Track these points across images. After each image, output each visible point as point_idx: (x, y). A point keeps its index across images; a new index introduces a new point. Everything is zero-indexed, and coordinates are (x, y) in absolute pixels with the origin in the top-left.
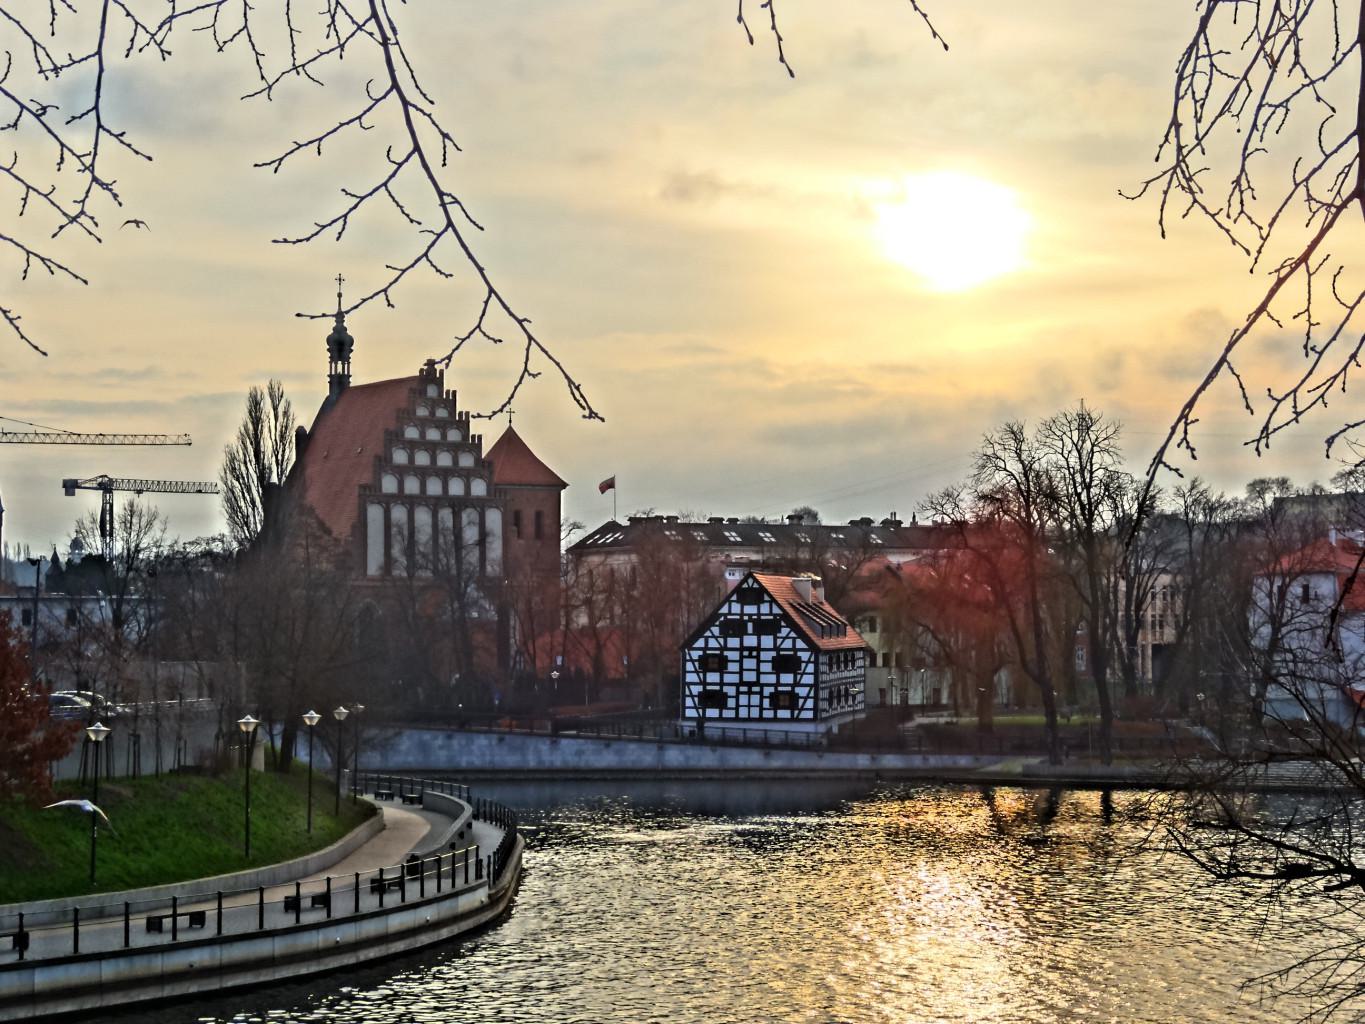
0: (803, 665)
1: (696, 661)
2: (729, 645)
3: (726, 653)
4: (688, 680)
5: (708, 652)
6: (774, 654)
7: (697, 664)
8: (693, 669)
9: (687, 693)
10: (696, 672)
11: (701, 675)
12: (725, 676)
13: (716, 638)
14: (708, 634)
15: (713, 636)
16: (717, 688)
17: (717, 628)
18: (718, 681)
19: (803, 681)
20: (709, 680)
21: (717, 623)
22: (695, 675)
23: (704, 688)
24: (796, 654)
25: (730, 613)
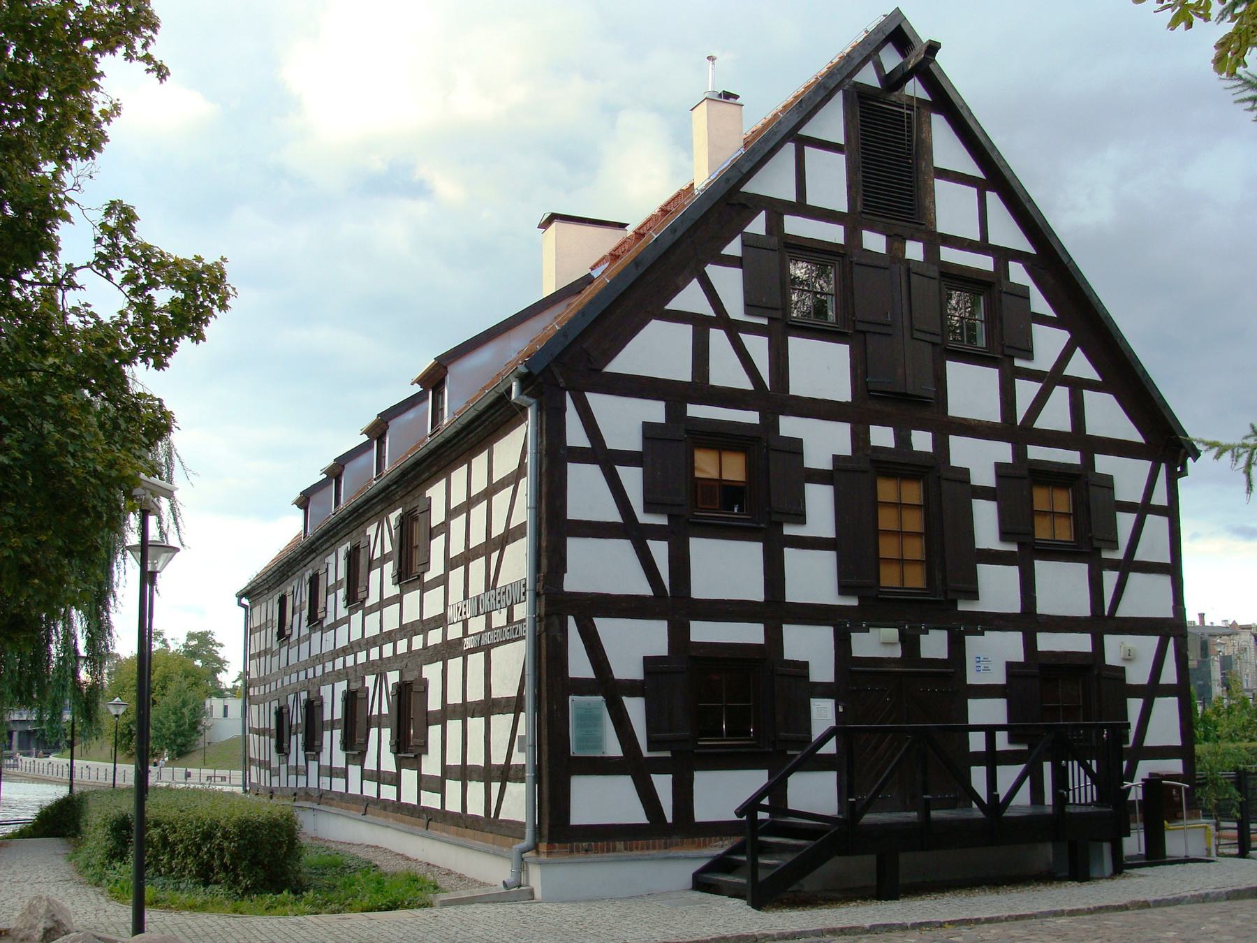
0: (1125, 522)
1: (628, 458)
2: (799, 386)
3: (789, 426)
4: (571, 583)
5: (694, 411)
6: (1003, 452)
7: (632, 478)
8: (613, 515)
9: (579, 665)
10: (628, 529)
11: (660, 550)
12: (789, 552)
13: (733, 330)
14: (691, 298)
15: (722, 320)
16: (752, 633)
17: (737, 273)
18: (756, 592)
19: (1124, 611)
20: (702, 587)
21: (734, 248)
22: (623, 549)
23: (678, 635)
24: (1088, 462)
25: (801, 208)
